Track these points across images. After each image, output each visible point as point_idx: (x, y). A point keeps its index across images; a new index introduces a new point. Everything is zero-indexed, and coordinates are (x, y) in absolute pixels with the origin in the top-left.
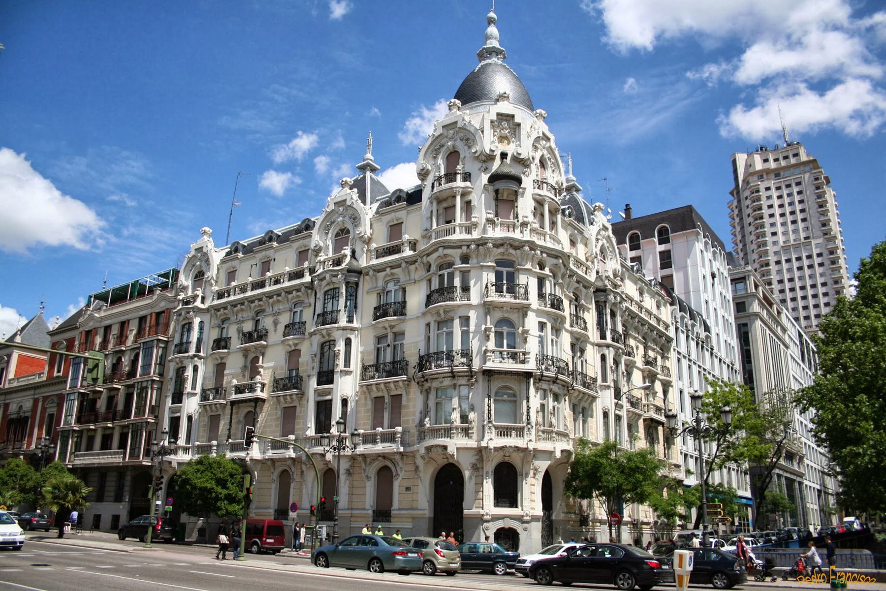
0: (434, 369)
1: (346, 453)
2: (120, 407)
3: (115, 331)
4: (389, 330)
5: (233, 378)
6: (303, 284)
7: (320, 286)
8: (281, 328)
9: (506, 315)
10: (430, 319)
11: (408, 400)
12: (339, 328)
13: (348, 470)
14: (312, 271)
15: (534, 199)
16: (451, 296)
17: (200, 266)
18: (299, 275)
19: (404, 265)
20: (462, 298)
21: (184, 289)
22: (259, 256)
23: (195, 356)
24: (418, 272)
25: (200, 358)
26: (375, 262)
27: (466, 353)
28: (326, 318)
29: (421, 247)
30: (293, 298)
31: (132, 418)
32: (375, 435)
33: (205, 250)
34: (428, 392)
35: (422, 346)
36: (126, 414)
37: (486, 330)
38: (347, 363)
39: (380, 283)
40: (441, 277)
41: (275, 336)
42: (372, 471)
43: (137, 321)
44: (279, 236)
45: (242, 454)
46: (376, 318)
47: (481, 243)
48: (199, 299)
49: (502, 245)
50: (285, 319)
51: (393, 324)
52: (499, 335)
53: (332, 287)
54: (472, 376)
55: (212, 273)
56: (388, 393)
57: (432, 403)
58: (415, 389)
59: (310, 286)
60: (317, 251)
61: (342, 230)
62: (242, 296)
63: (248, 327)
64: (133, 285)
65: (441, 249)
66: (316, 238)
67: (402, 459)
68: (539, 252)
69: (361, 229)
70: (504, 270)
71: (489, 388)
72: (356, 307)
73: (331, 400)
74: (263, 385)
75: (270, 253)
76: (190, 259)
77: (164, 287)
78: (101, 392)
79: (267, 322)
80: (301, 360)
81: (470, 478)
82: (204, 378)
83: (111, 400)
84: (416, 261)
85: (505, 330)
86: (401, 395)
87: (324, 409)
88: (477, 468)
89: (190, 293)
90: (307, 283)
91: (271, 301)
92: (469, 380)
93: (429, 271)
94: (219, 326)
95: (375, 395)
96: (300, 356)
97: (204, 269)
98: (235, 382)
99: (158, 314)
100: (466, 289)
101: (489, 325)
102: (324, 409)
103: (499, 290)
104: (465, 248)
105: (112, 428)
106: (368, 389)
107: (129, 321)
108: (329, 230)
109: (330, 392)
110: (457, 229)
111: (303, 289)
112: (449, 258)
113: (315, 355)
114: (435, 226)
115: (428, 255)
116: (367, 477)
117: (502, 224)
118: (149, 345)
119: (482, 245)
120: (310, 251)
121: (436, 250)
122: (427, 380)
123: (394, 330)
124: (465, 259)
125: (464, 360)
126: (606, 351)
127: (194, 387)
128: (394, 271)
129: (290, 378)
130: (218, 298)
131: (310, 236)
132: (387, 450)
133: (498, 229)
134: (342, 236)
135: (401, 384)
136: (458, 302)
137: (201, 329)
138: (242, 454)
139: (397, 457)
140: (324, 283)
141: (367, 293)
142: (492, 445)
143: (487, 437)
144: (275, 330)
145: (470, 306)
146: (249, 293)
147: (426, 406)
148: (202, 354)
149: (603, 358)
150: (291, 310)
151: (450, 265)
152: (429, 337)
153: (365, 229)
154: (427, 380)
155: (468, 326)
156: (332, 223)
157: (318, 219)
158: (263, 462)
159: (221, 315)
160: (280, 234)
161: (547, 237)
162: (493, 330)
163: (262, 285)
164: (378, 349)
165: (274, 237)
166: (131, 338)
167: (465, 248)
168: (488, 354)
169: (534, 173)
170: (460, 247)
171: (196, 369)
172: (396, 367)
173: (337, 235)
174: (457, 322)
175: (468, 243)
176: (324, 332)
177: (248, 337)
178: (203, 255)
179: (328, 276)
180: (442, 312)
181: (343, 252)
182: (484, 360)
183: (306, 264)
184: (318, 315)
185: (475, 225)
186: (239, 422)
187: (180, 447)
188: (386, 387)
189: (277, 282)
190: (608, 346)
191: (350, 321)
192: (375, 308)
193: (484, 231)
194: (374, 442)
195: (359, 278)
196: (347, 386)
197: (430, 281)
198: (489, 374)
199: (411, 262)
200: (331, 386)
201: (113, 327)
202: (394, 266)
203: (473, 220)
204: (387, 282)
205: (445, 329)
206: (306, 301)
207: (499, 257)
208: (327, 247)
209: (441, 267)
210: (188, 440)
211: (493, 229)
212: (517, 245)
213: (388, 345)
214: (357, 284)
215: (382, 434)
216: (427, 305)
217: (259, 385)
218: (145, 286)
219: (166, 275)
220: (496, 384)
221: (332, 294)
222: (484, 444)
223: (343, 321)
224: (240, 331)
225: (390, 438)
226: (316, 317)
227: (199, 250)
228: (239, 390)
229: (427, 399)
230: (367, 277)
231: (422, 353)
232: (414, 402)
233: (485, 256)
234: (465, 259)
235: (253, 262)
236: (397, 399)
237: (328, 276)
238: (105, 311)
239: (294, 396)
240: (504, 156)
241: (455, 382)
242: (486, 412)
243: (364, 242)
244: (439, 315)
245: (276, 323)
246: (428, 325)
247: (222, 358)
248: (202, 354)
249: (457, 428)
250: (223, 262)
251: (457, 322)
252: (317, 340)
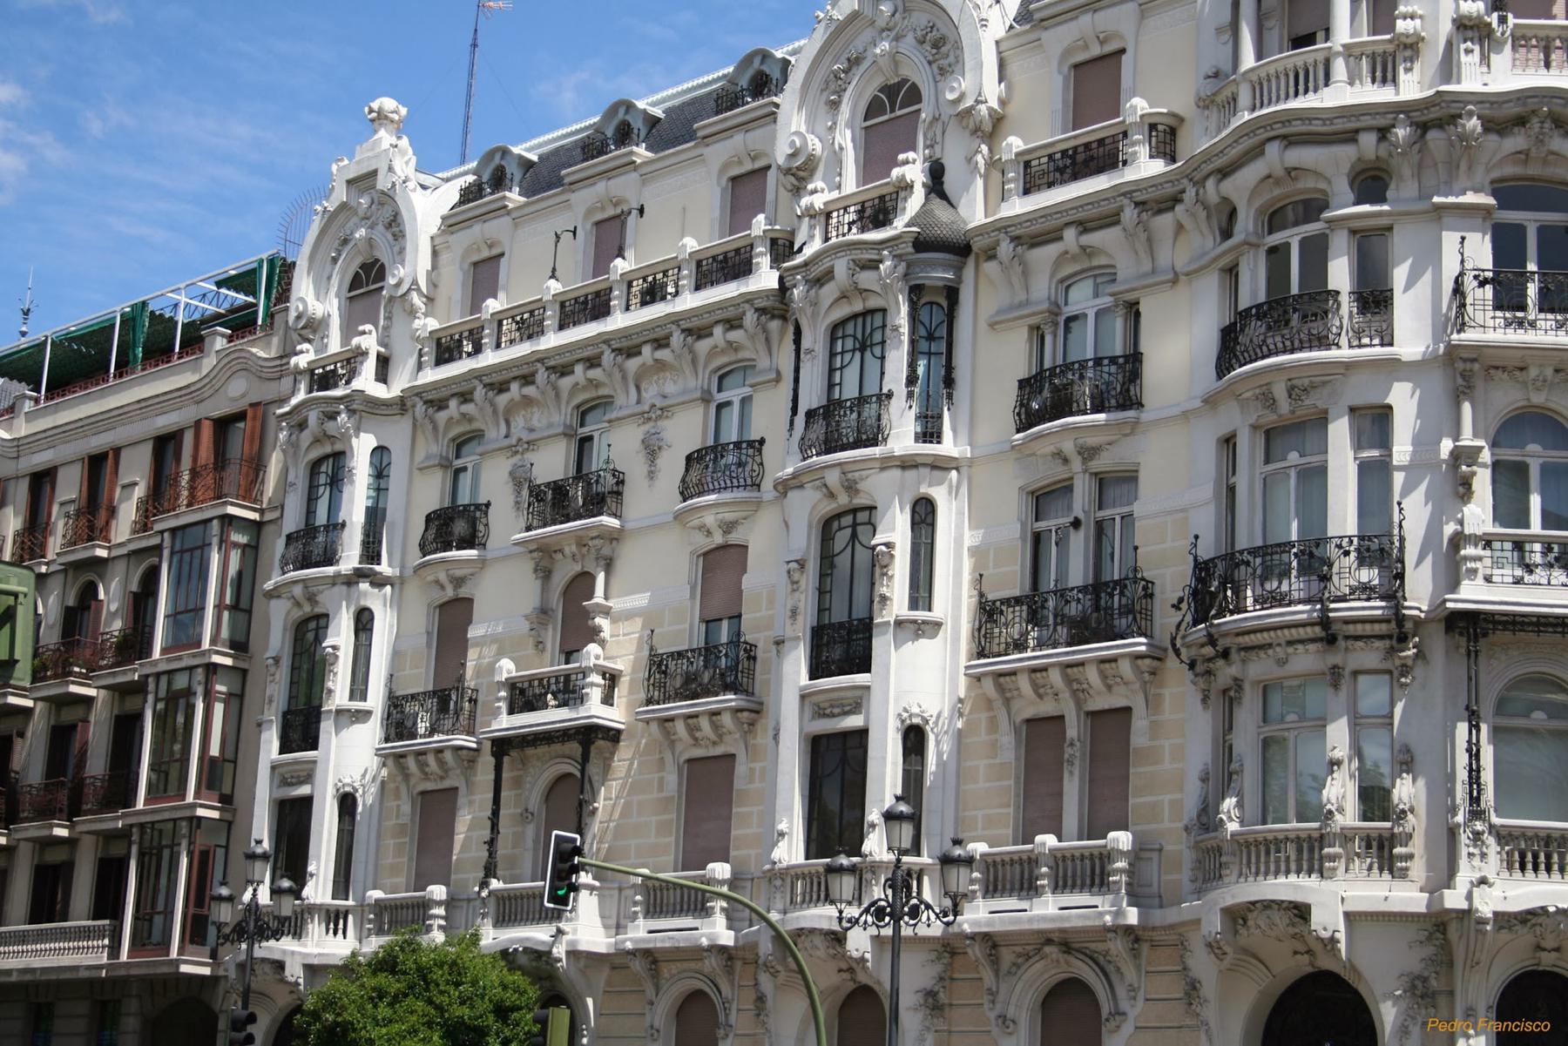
0: (1253, 613)
1: (922, 931)
2: (97, 765)
3: (69, 487)
4: (1077, 464)
5: (500, 654)
6: (748, 299)
7: (815, 304)
8: (672, 466)
9: (1538, 399)
10: (1234, 418)
11: (1155, 729)
12: (887, 463)
13: (930, 994)
14: (782, 248)
16: (1316, 327)
17: (370, 241)
18: (734, 265)
19: (1129, 214)
20: (1359, 334)
21: (313, 328)
22: (583, 198)
23: (359, 575)
24: (1185, 241)
25: (379, 582)
26: (1018, 206)
27: (1379, 549)
28: (840, 424)
29: (1198, 142)
30: (713, 352)
31: (140, 805)
32: (1032, 861)
33: (382, 183)
34: (1230, 698)
35: (1205, 523)
36: (119, 790)
37: (1462, 456)
38: (921, 590)
39: (1042, 288)
40: (1277, 255)
41: (652, 497)
42: (1022, 995)
43: (146, 451)
44: (653, 122)
45: (539, 934)
46: (1027, 419)
47: (1435, 117)
48: (369, 367)
49: (1521, 121)
50: (686, 432)
51: (1092, 441)
52: (1511, 479)
53: (858, 307)
54: (1403, 639)
55: (414, 266)
56: (1079, 704)
57: (1246, 742)
58: (1179, 687)
59: (778, 306)
60: (800, 173)
61: (891, 91)
62: (524, 349)
63: (552, 464)
64: (129, 321)
65: (1273, 149)
66: (794, 124)
67: (1135, 954)
69: (965, 84)
70: (1531, 221)
71: (1473, 680)
72: (949, 382)
73: (863, 733)
74: (612, 679)
75: (625, 187)
76: (331, 218)
77: (241, 323)
78: (27, 712)
79: (619, 446)
80: (747, 582)
81: (1403, 1031)
82: (396, 655)
83: (62, 738)
84: (1176, 199)
85: (1535, 455)
86: (1128, 710)
87: (836, 763)
88: (1427, 995)
89: (334, 345)
90: (766, 293)
91: (633, 364)
92: (1392, 651)
93: (1227, 234)
94: (444, 464)
95: (1029, 713)
96: (744, 571)
97: (384, 256)
98: (507, 668)
99: (223, 425)
100: (1375, 299)
101: (1467, 440)
102: (836, 763)
103: (1508, 299)
104: (1368, 140)
105: (70, 842)
106: (1001, 689)
107: (117, 451)
108: (840, 92)
109: (856, 701)
110: (1340, 68)
111: (750, 318)
112: (1309, 183)
113: (802, 564)
114: (1248, 60)
115: (1224, 173)
116: (1003, 1018)
117: (1520, 40)
118: (192, 539)
119: (1440, 124)
120: (772, 175)
121: (1257, 152)
122: (1225, 654)
123: (1102, 463)
124: (1371, 183)
125: (1369, 575)
127: (359, 689)
128: (1087, 239)
129: (710, 651)
130: (440, 361)
131: (772, 117)
132: (1076, 919)
133: (1502, 59)
134: (892, 112)
135: (1125, 667)
136: (1343, 353)
137: (380, 473)
138: (539, 934)
139: (1117, 946)
140: (829, 292)
141: (992, 325)
142: (1488, 904)
143: (1465, 876)
144: (651, 475)
145: (1394, 368)
146: (552, 340)
147: (1225, 752)
148: (384, 568)
150: (706, 399)
151: (1312, 208)
152: (1231, 490)
153: (981, 82)
154: (1225, 654)
155: (1385, 441)
156: (854, 62)
157: (799, 51)
158: (616, 962)
159: (451, 420)
160: (658, 112)
162: (1486, 456)
163: (594, 306)
164: (1037, 539)
165: (638, 124)
166: (128, 512)
167: (1368, 140)
168: (1469, 551)
170: (1350, 137)
171: (364, 622)
172: (1108, 606)
173: (873, 109)
174: (1340, 431)
175: (1380, 120)
176: (833, 478)
177: (553, 501)
178: (377, 203)
179: (841, 267)
180: (1280, 391)
181: (896, 172)
182: (1452, 572)
183: (760, 224)
184: (810, 414)
185: (1411, 48)
186: (526, 816)
187: (312, 909)
188: (1069, 681)
189: (653, 294)
191: (930, 433)
192: (1022, 384)
193: (1448, 68)
194: (1028, 888)
195: (959, 270)
196: (921, 677)
197: (1232, 272)
198: (1471, 627)
199: (1156, 201)
200: (860, 678)
201: (62, 475)
202: (1094, 217)
203: (1401, 26)
204: (1066, 284)
205: (1293, 457)
206: (763, 362)
207: (1510, 170)
208: (837, 157)
209: (1275, 219)
210: (342, 883)
211: (1485, 60)
213: (1076, 524)
214: (952, 293)
215: (1059, 859)
216: (1224, 364)
217: (596, 678)
218: (172, 322)
219: (243, 281)
220: (1501, 668)
221: (860, 333)
222: (1454, 899)
223: (902, 436)
224: (519, 479)
225: (1086, 873)
226: (800, 420)
227: (363, 182)
228: (523, 697)
229: (1229, 726)
230: (990, 267)
231: (1206, 551)
232: (1176, 737)
233: (1452, 167)
234: (1371, 183)
235: (562, 222)
236: (1111, 725)
237: (841, 267)
238: (30, 417)
239: (726, 719)
241: (1335, 659)
242: (1462, 775)
243: (976, 131)
244: (1269, 400)
245: (652, 450)
246: (1229, 442)
247: (458, 582)
248: (384, 568)
249: (1346, 837)
250: (451, 224)
251: (1340, 431)
252: (806, 507)
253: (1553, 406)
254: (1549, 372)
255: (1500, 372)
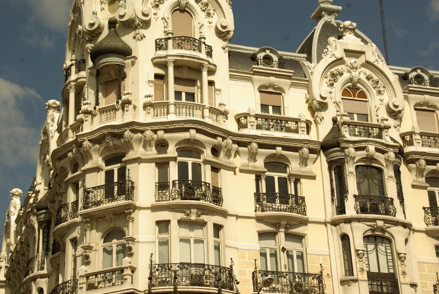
9: (112, 225)
15: (156, 65)
68: (149, 133)
70: (115, 167)
104: (70, 154)
126: (346, 228)
133: (97, 119)
149: (345, 238)
161: (172, 108)
169: (156, 31)
190: (348, 221)
207: (107, 154)
212: (116, 133)
234: (75, 168)
240: (112, 23)
253: (116, 226)
254: (111, 216)
255: (100, 219)
